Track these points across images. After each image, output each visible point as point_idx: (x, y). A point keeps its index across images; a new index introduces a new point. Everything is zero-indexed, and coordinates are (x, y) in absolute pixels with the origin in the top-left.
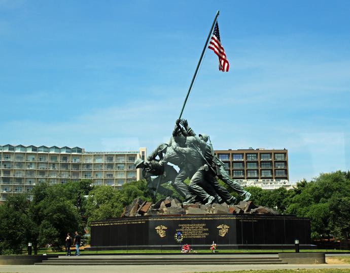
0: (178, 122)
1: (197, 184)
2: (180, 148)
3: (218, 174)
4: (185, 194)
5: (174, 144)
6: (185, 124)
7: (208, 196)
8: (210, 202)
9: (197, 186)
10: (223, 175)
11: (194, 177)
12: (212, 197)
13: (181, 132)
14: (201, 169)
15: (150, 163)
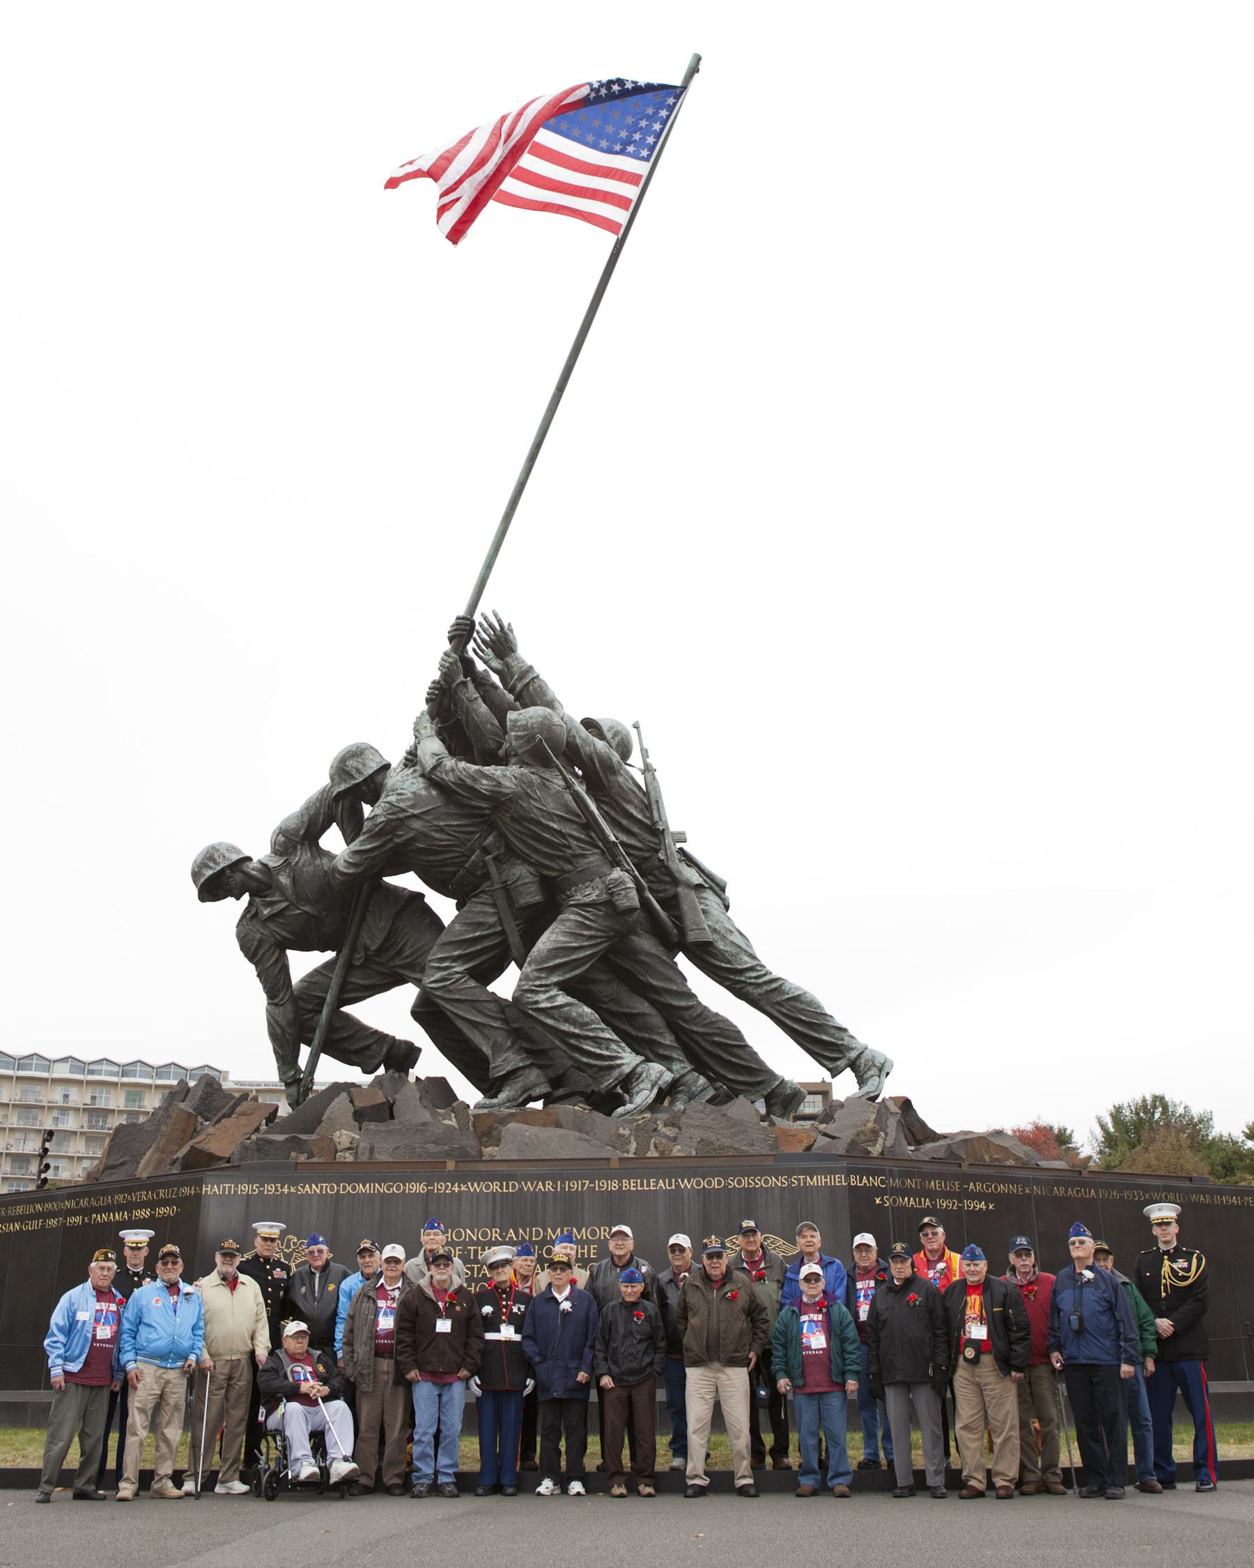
0: (462, 631)
1: (565, 987)
2: (462, 764)
3: (692, 937)
4: (486, 1049)
5: (433, 747)
6: (502, 644)
7: (629, 1059)
8: (644, 1095)
9: (562, 999)
10: (721, 945)
11: (545, 942)
12: (656, 1068)
13: (478, 692)
14: (591, 893)
15: (287, 863)
